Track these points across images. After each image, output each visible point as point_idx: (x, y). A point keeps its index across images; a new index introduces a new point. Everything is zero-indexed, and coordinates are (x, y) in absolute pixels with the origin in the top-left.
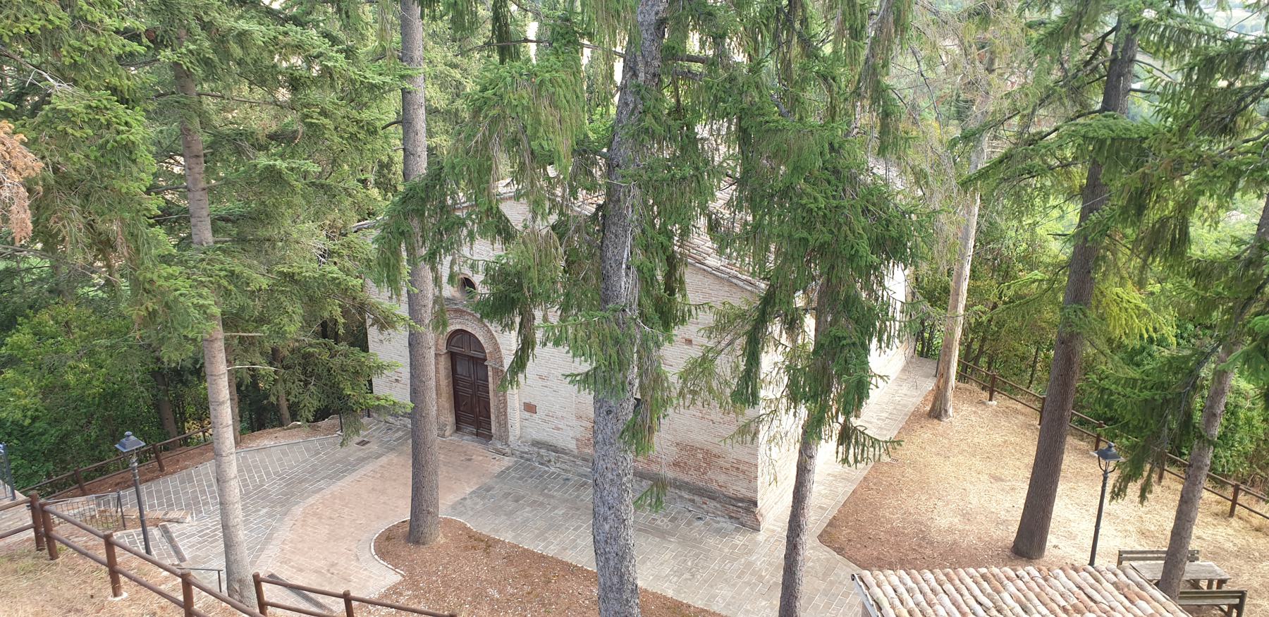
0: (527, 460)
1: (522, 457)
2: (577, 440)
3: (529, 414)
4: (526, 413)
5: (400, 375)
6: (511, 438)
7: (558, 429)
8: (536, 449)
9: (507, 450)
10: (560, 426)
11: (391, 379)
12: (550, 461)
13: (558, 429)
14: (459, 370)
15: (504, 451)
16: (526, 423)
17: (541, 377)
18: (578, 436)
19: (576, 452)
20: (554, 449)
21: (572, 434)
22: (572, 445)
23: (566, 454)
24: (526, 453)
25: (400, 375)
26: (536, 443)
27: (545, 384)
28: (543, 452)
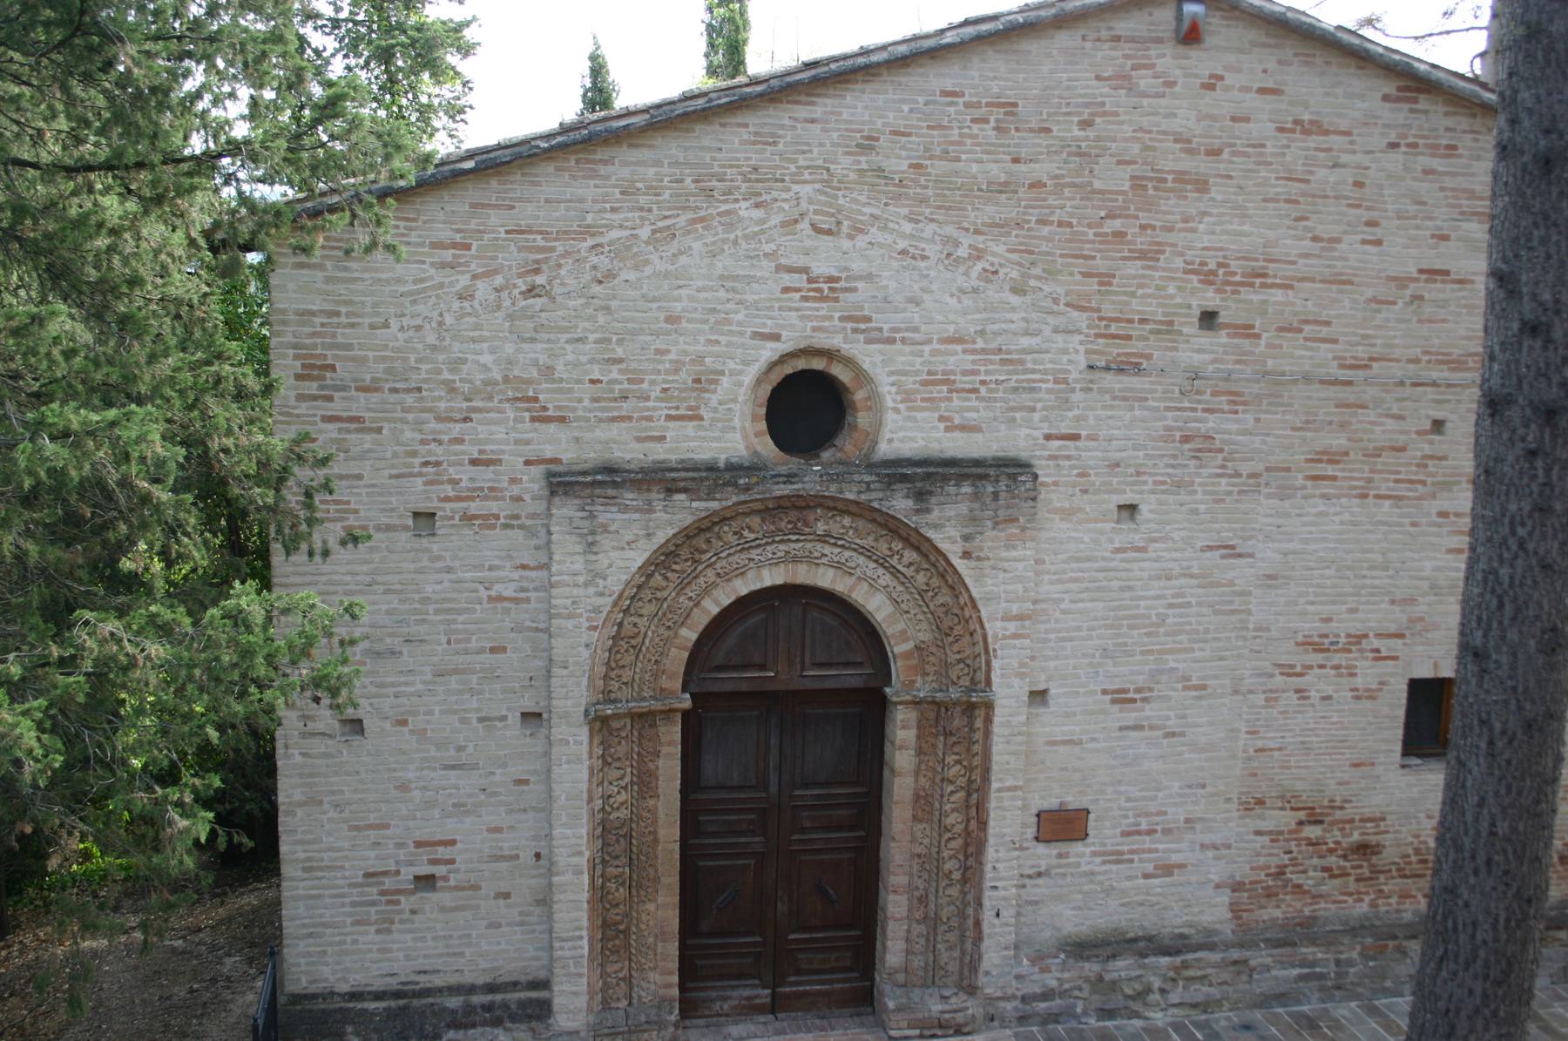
0: (1054, 1018)
1: (1023, 1019)
2: (1237, 887)
3: (1054, 849)
4: (1041, 849)
5: (442, 852)
6: (993, 956)
7: (1167, 870)
8: (1091, 968)
9: (973, 1008)
10: (1175, 858)
11: (388, 883)
12: (1142, 995)
13: (1167, 870)
14: (712, 768)
15: (960, 1018)
16: (1040, 888)
17: (1121, 698)
18: (1242, 871)
19: (1227, 930)
20: (1146, 945)
21: (1217, 871)
22: (1214, 912)
23: (1201, 947)
24: (1047, 995)
25: (442, 852)
26: (1080, 948)
27: (1131, 717)
28: (1122, 967)
